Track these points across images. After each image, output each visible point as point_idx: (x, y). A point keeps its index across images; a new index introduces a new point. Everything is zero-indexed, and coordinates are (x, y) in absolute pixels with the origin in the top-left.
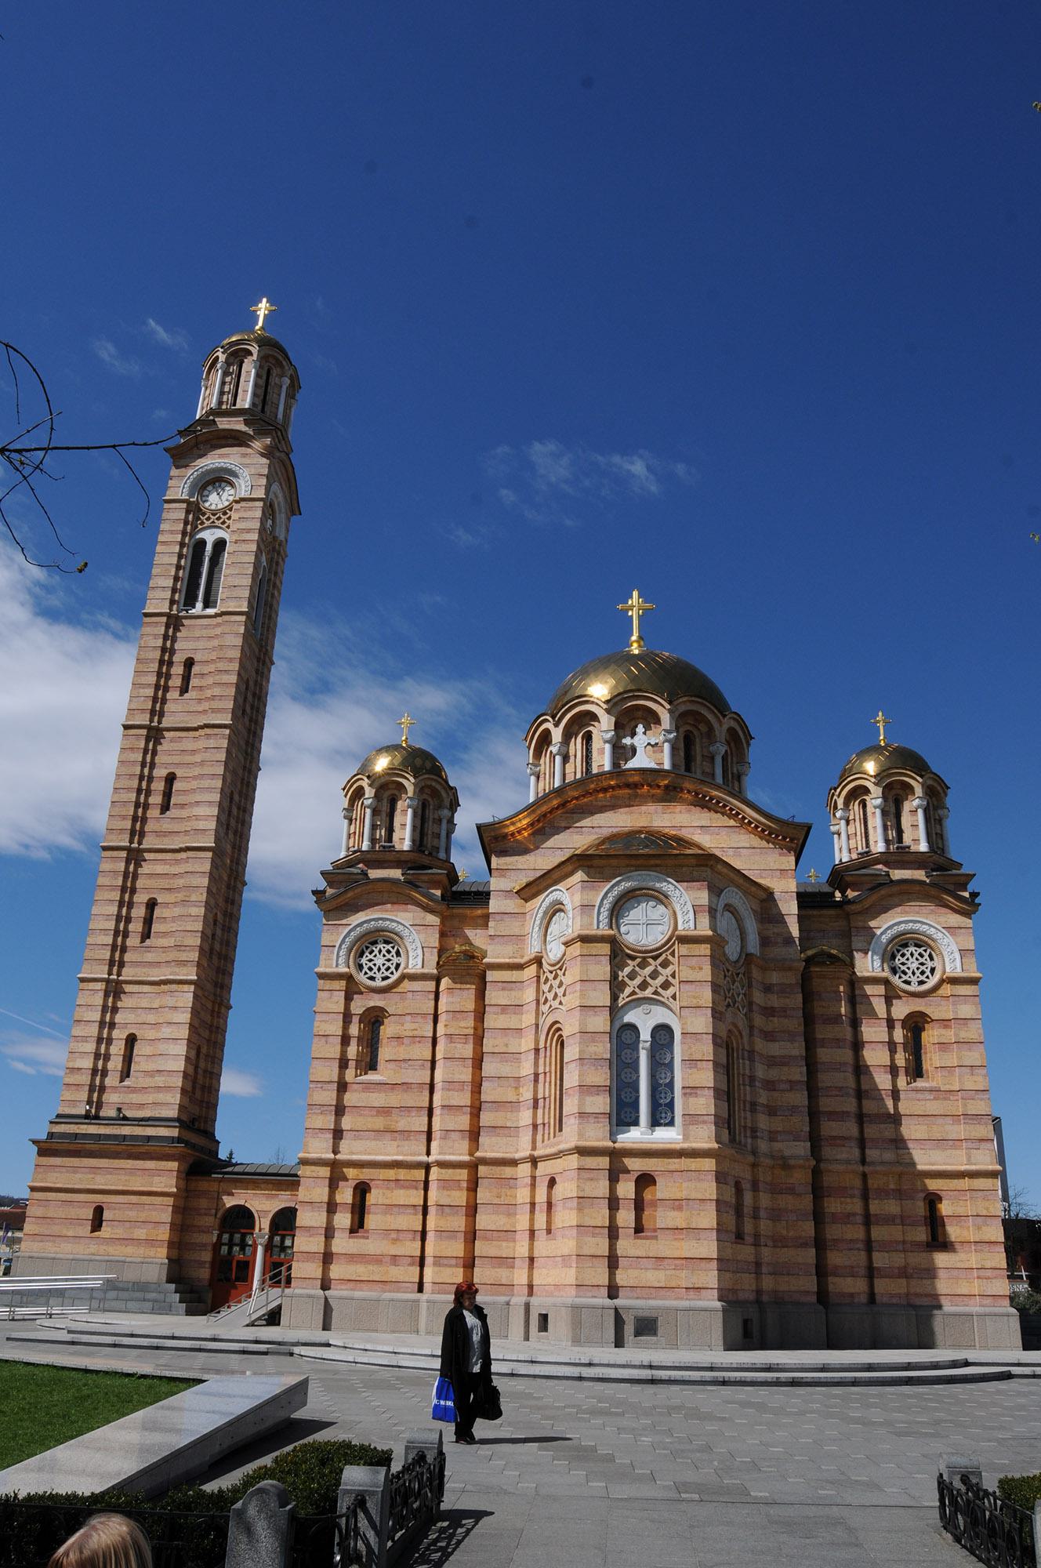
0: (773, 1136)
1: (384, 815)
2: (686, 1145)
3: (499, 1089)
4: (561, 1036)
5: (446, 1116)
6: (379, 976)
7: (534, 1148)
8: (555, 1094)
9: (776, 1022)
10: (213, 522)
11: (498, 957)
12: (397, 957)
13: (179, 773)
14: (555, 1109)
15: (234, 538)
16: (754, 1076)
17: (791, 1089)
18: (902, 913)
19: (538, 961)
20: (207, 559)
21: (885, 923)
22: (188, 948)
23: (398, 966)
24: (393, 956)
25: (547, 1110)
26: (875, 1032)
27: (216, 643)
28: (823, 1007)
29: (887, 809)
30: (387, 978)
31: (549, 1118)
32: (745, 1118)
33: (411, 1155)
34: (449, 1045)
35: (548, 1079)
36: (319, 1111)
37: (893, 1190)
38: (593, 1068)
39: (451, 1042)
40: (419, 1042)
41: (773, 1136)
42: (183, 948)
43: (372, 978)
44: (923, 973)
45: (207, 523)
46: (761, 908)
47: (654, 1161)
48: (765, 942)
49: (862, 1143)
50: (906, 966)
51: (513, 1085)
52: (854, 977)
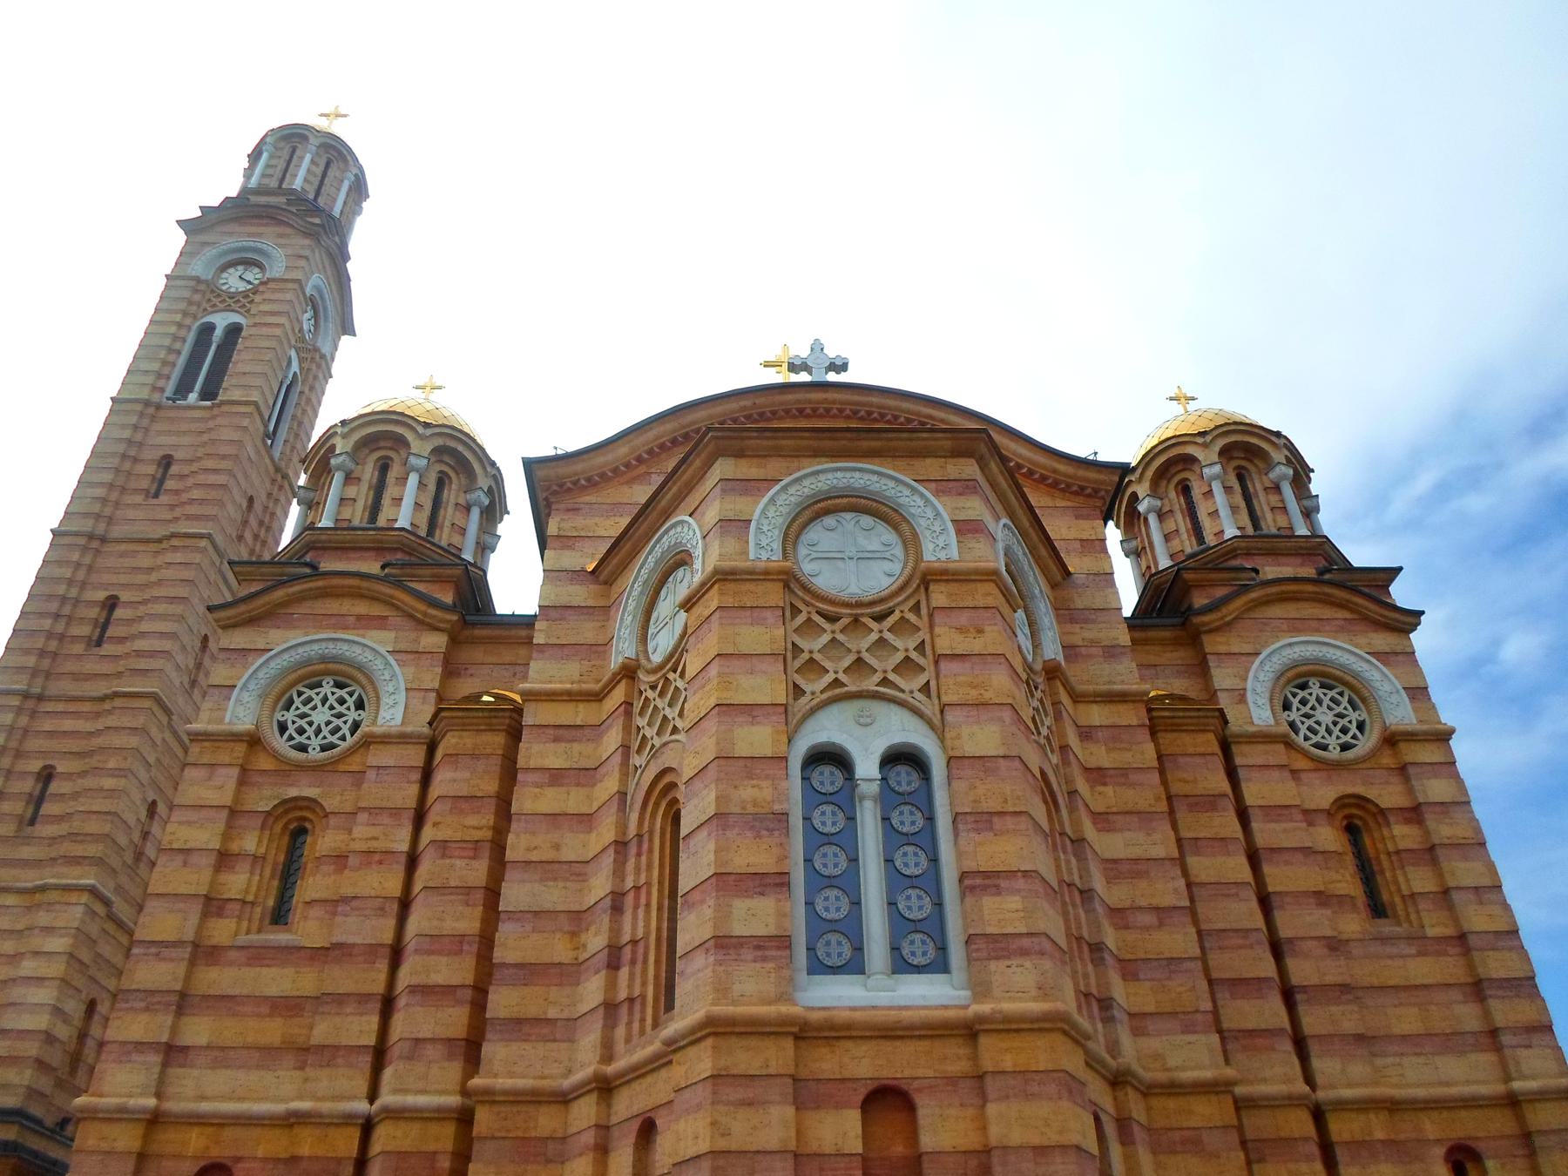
0: (1139, 1022)
1: (364, 486)
2: (985, 1008)
3: (535, 936)
4: (675, 801)
5: (419, 1009)
6: (315, 743)
7: (608, 1057)
8: (659, 929)
9: (1107, 797)
10: (229, 305)
11: (550, 682)
12: (357, 709)
13: (125, 596)
14: (657, 962)
15: (252, 321)
16: (1091, 890)
17: (1161, 924)
18: (1289, 631)
19: (629, 672)
20: (213, 348)
21: (1266, 645)
22: (89, 838)
23: (356, 726)
24: (348, 709)
25: (639, 967)
26: (1285, 831)
27: (205, 437)
28: (1186, 782)
29: (1229, 484)
30: (332, 746)
31: (644, 984)
32: (1086, 976)
33: (335, 1098)
34: (438, 862)
35: (643, 901)
36: (143, 1004)
37: (1382, 1142)
38: (749, 834)
39: (444, 856)
40: (380, 862)
41: (1139, 1022)
42: (79, 838)
43: (303, 748)
44: (1344, 731)
45: (222, 306)
46: (1055, 598)
47: (907, 1049)
48: (1069, 649)
49: (1300, 1045)
50: (1314, 719)
51: (567, 928)
52: (1228, 732)
